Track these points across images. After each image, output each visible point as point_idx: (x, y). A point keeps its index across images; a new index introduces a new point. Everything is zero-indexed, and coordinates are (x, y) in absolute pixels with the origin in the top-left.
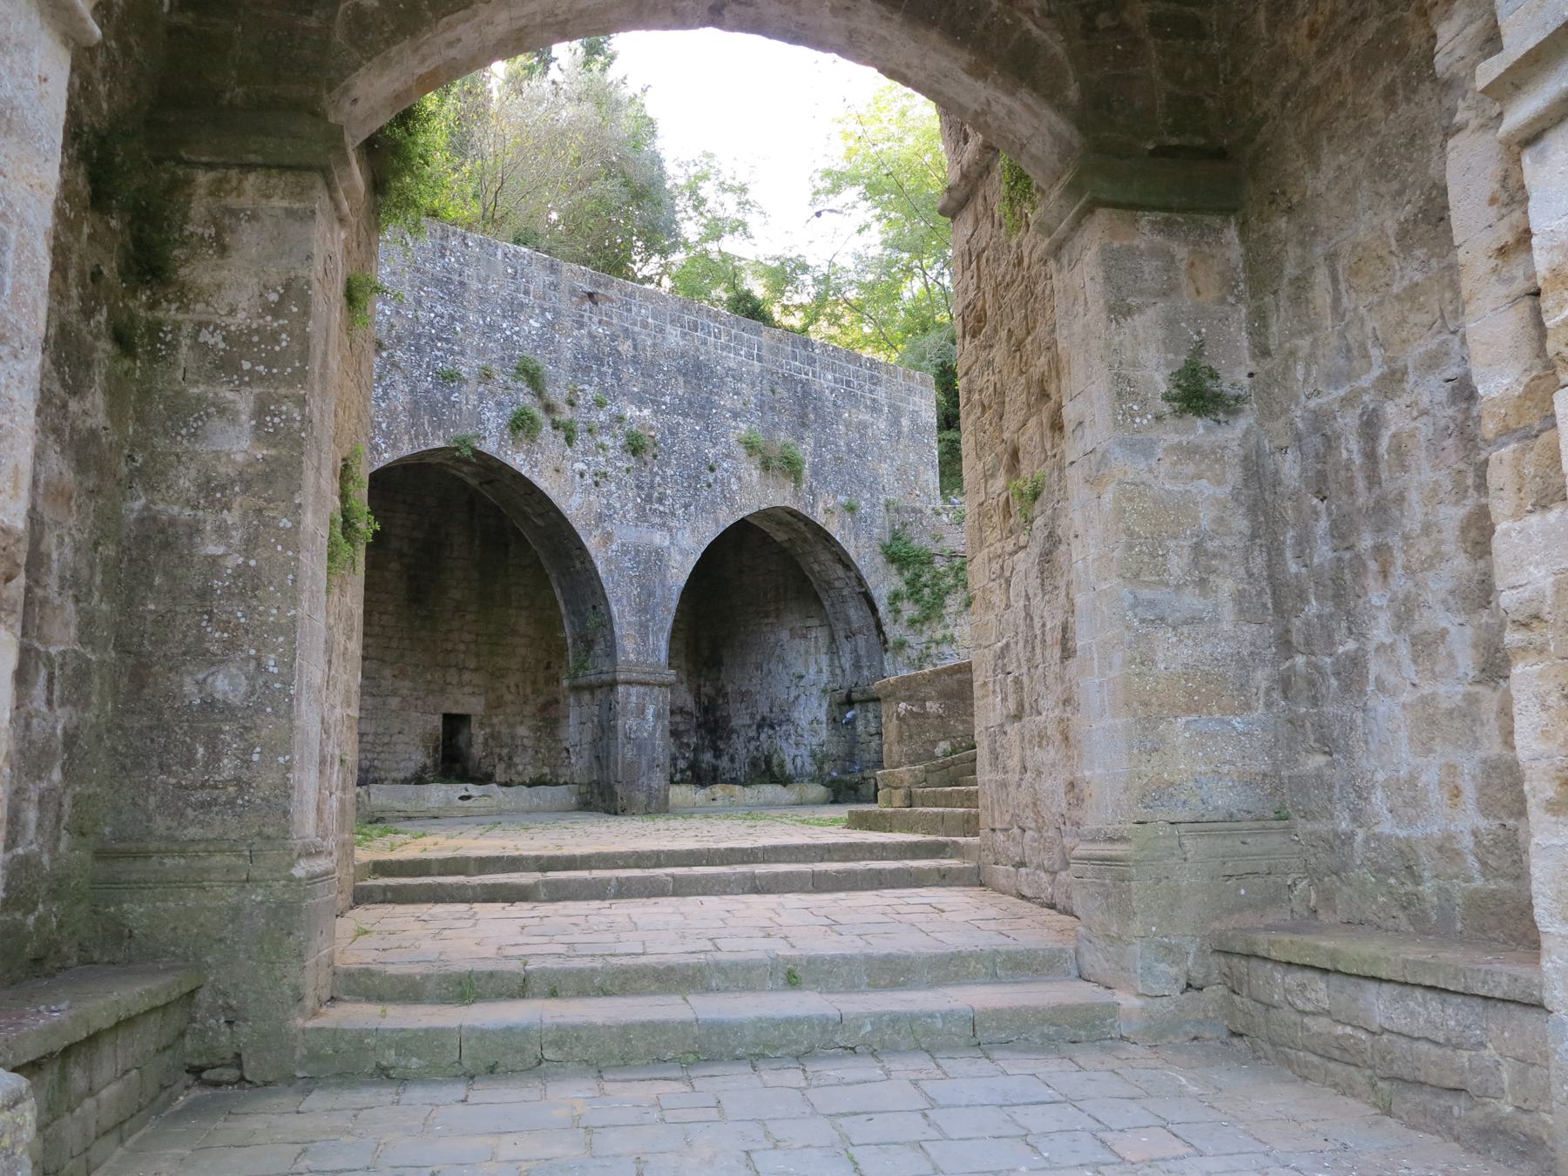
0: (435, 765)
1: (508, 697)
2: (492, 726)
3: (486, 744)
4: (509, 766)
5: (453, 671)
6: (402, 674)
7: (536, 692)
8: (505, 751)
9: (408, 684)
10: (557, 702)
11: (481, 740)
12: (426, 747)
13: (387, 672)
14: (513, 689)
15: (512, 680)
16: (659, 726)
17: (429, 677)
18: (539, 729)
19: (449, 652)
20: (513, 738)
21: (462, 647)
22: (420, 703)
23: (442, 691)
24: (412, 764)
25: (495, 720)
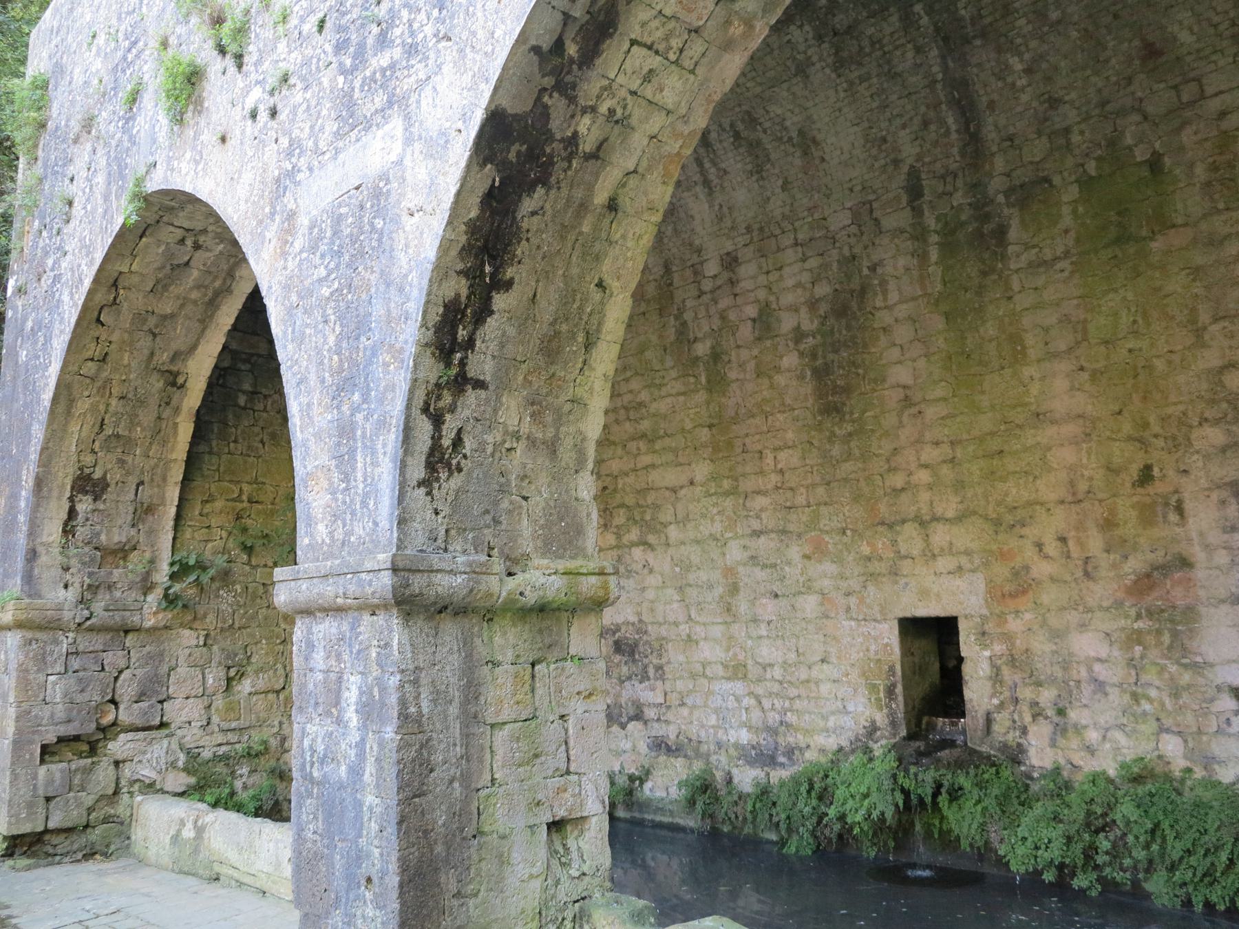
0: (893, 724)
1: (1042, 569)
2: (1008, 638)
3: (996, 677)
4: (1061, 730)
5: (910, 529)
6: (818, 552)
7: (1119, 546)
8: (1047, 696)
9: (830, 567)
10: (1185, 563)
11: (984, 669)
12: (873, 688)
13: (794, 552)
14: (1052, 548)
15: (1049, 526)
16: (371, 743)
17: (866, 550)
18: (1136, 637)
19: (897, 492)
20: (1066, 667)
21: (924, 476)
22: (853, 601)
23: (894, 573)
24: (848, 722)
25: (1014, 625)
